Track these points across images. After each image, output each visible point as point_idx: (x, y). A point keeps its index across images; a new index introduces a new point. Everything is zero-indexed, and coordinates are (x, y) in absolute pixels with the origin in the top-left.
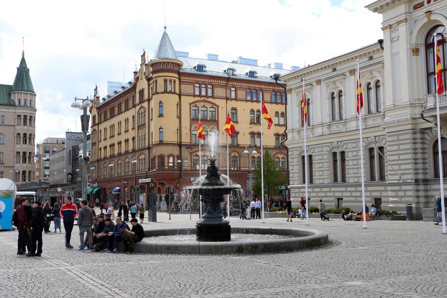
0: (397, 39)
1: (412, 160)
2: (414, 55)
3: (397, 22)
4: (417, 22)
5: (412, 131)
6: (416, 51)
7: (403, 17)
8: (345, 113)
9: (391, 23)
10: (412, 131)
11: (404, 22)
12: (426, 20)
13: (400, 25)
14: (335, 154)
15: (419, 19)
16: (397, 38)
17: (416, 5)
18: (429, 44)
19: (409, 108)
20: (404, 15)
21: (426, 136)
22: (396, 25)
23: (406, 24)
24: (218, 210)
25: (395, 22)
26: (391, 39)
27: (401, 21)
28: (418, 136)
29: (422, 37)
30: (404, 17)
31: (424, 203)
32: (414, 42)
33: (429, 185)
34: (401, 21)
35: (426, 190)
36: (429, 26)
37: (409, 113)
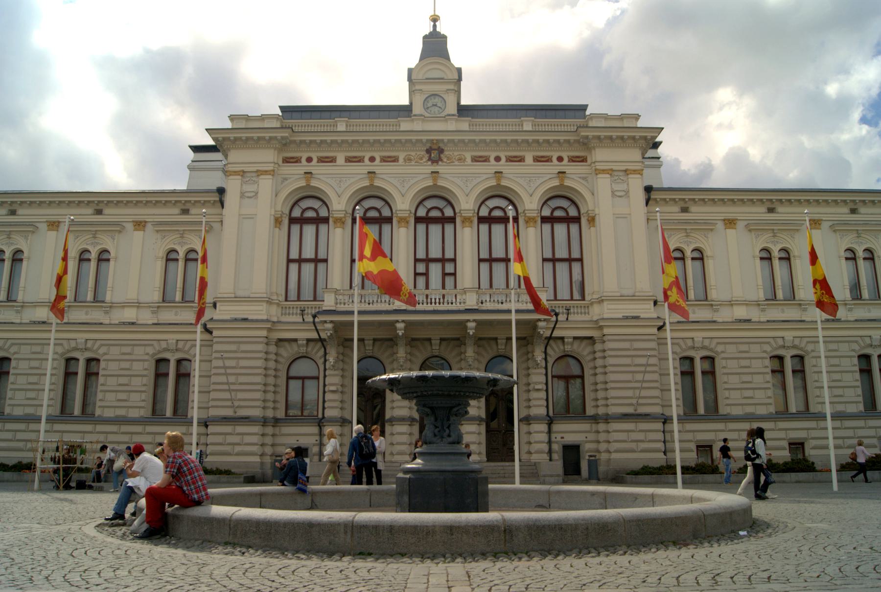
0: (254, 196)
1: (261, 386)
2: (276, 227)
3: (257, 171)
4: (286, 183)
5: (265, 340)
6: (278, 222)
7: (270, 167)
8: (24, 291)
9: (246, 169)
10: (265, 340)
11: (270, 174)
12: (303, 183)
13: (262, 177)
14: (161, 362)
15: (290, 178)
16: (254, 194)
17: (287, 158)
18: (384, 217)
19: (265, 304)
20: (273, 165)
21: (283, 352)
22: (254, 174)
23: (273, 179)
24: (449, 436)
25: (255, 169)
26: (241, 193)
27: (266, 172)
28: (273, 348)
29: (289, 203)
30: (272, 168)
31: (270, 456)
32: (279, 208)
33: (278, 428)
34: (266, 172)
35: (273, 435)
36: (300, 194)
37: (264, 312)
